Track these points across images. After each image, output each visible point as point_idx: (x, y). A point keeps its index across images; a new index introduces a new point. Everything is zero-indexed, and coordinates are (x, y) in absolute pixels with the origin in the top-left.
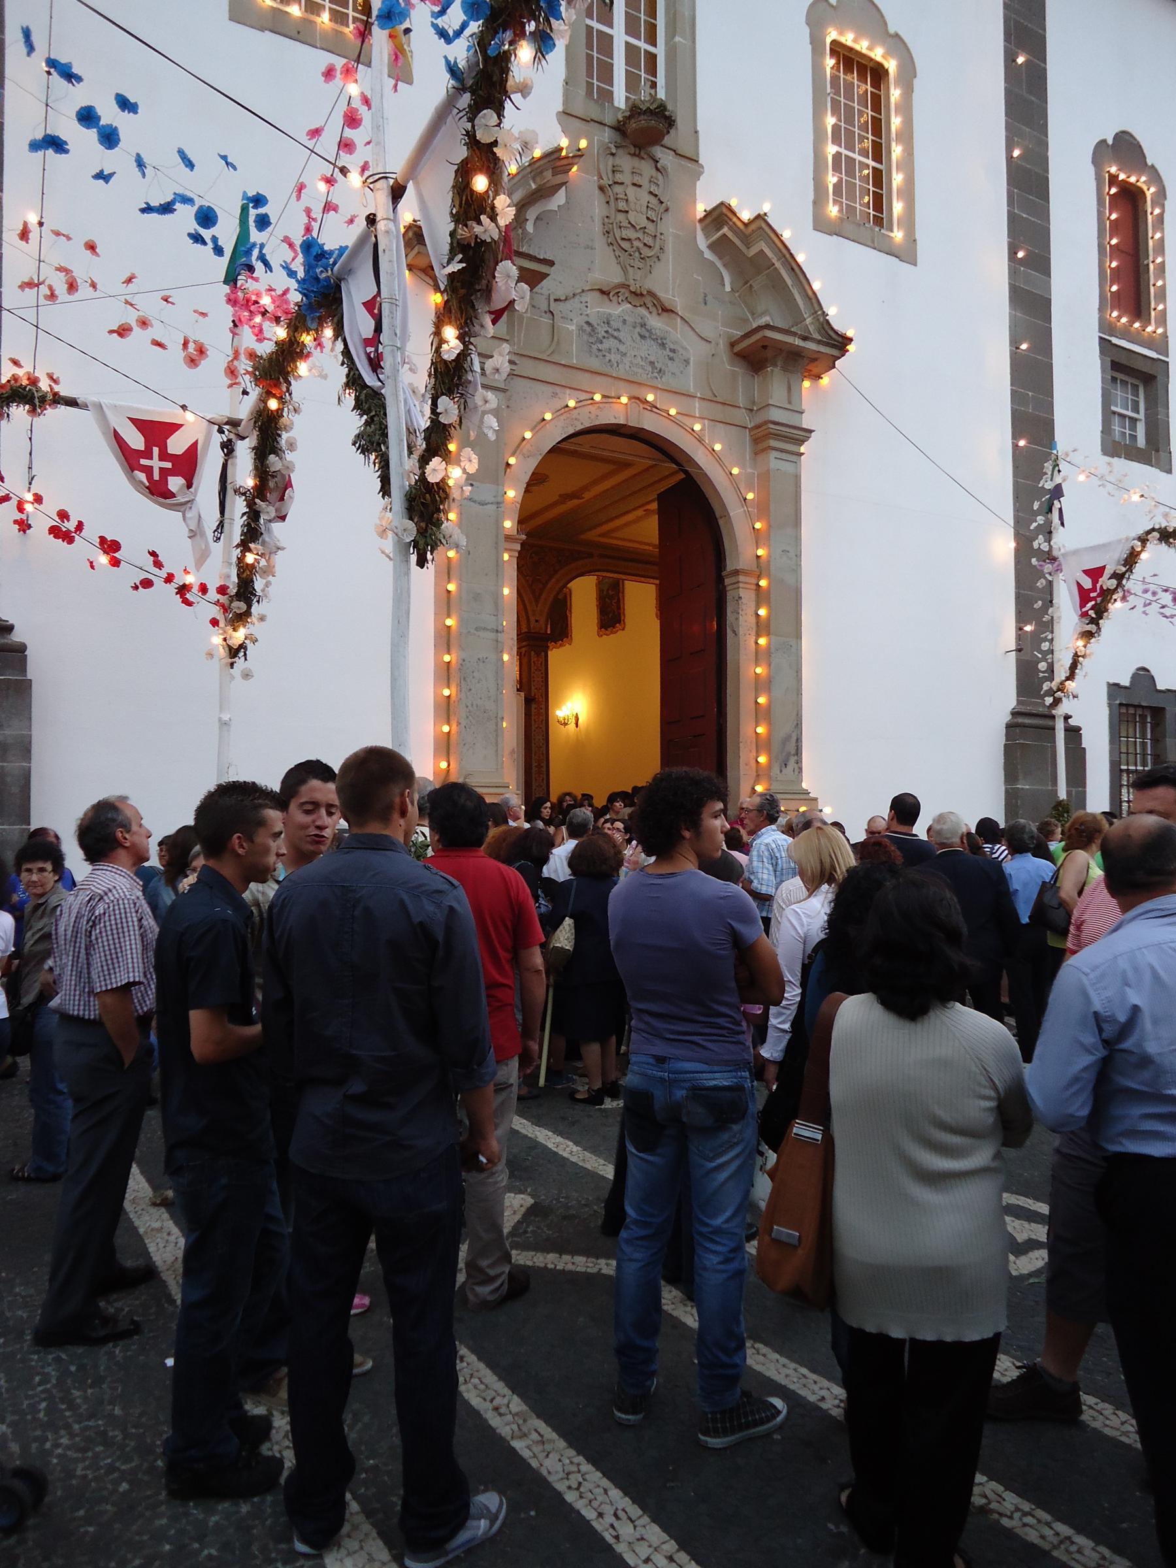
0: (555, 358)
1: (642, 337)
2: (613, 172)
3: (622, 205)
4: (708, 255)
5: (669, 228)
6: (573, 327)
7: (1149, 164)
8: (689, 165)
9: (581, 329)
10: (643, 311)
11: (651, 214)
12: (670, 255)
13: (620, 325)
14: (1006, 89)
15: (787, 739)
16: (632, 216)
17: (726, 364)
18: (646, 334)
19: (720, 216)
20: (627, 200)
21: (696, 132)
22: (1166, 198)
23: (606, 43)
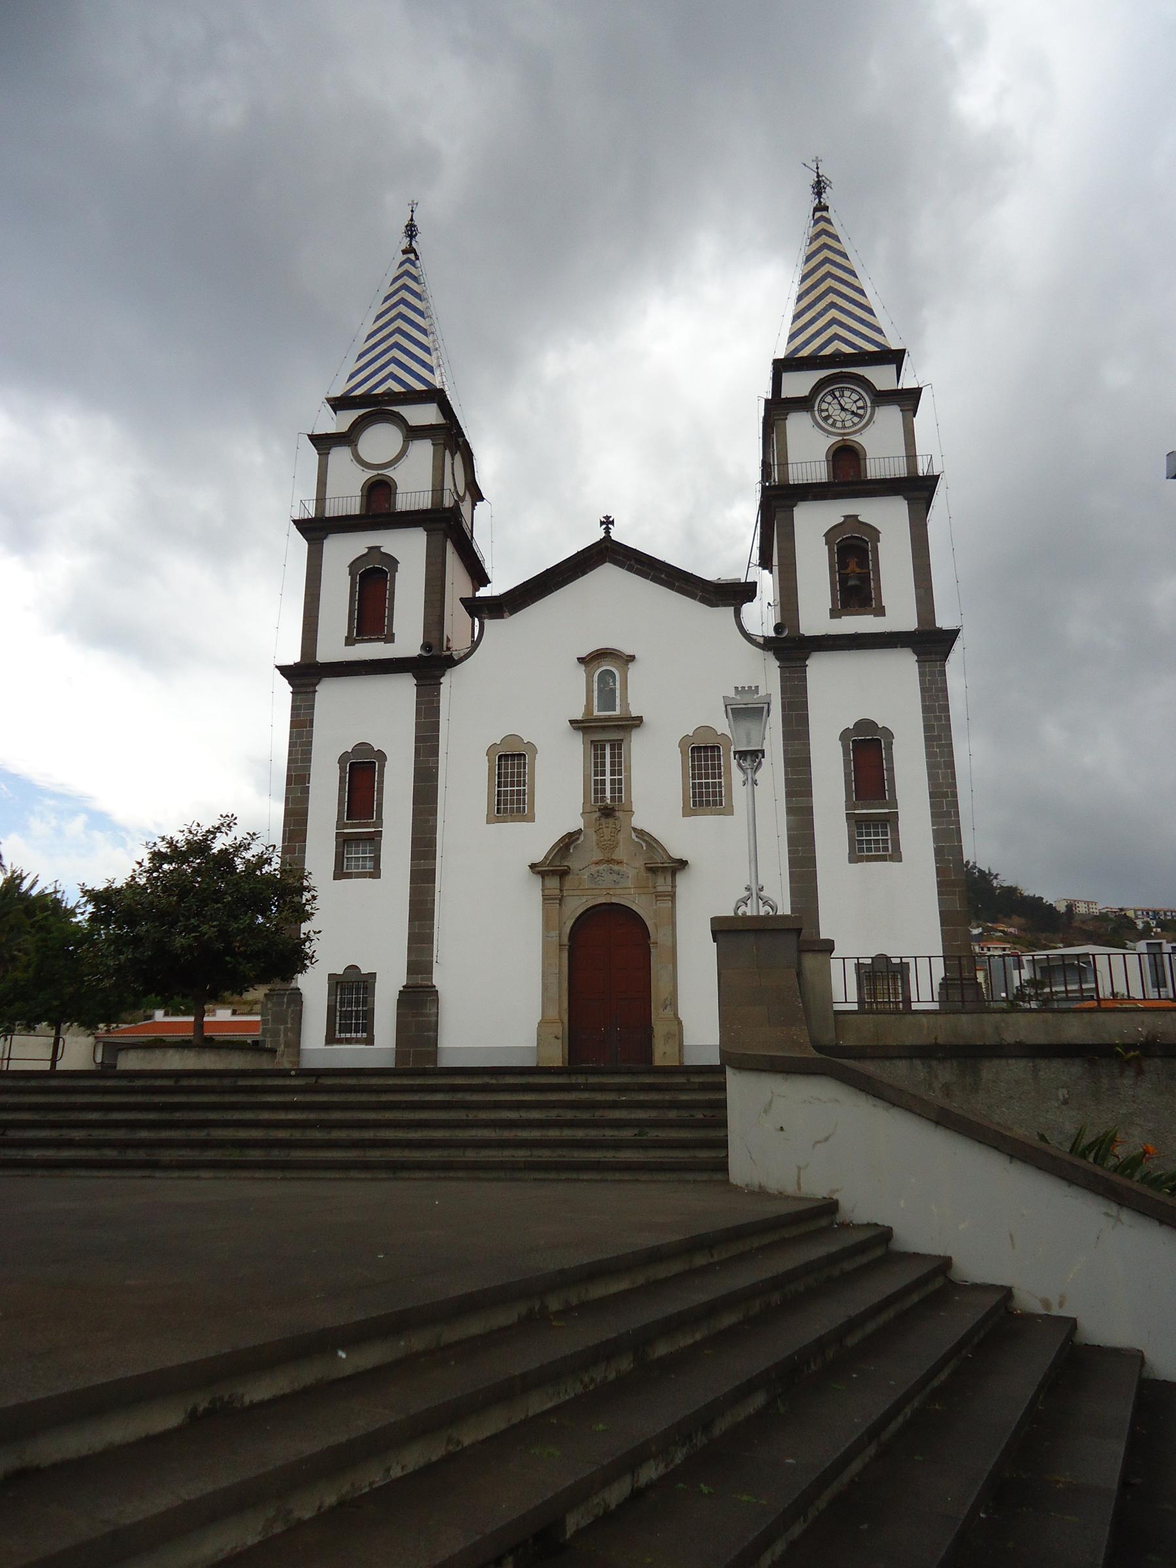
0: (580, 887)
1: (611, 873)
2: (599, 825)
3: (602, 835)
4: (636, 840)
5: (621, 836)
6: (586, 877)
7: (880, 726)
8: (629, 813)
9: (588, 876)
10: (611, 865)
11: (613, 834)
12: (621, 844)
13: (603, 872)
14: (784, 732)
15: (667, 998)
16: (605, 838)
17: (644, 874)
18: (612, 872)
19: (635, 829)
20: (603, 833)
21: (631, 802)
22: (893, 738)
23: (603, 782)
